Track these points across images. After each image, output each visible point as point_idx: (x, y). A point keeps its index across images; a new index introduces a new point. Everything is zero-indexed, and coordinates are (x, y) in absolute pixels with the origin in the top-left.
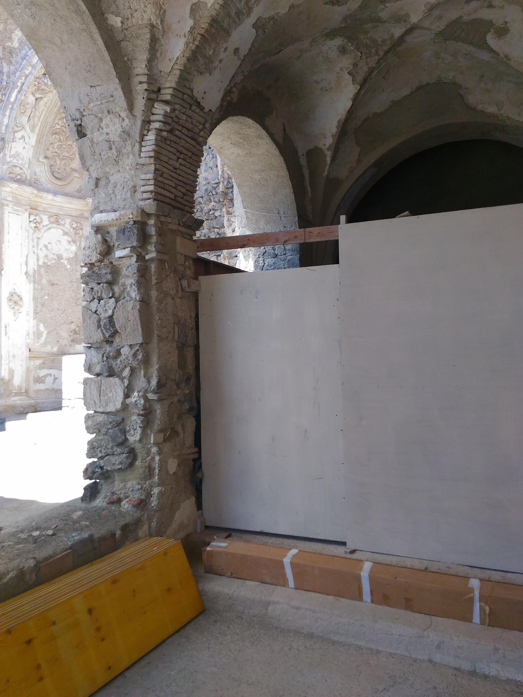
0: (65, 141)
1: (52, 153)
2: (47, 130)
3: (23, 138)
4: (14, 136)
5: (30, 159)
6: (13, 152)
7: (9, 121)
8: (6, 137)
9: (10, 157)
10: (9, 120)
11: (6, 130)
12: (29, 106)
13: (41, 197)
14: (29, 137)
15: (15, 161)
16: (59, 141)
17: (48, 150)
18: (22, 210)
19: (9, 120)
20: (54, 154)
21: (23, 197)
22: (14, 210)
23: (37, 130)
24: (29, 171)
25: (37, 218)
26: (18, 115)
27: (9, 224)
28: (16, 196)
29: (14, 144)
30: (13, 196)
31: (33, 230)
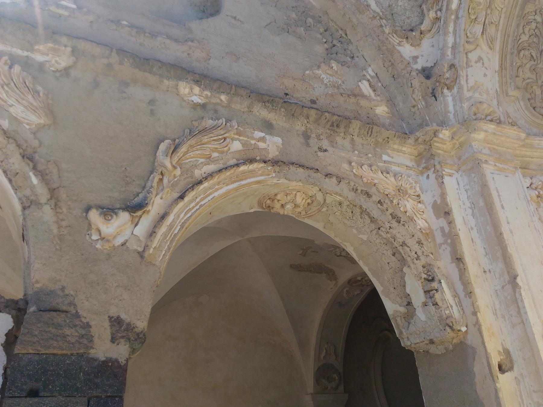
0: (539, 58)
1: (524, 80)
2: (509, 47)
3: (481, 61)
4: (467, 58)
5: (497, 90)
6: (471, 83)
7: (455, 39)
8: (456, 62)
9: (468, 91)
10: (455, 37)
11: (454, 54)
12: (481, 7)
13: (531, 147)
14: (489, 60)
15: (477, 95)
16: (530, 60)
17: (517, 76)
18: (509, 168)
19: (455, 37)
20: (529, 81)
21: (504, 149)
22: (497, 170)
23: (498, 45)
24: (501, 109)
25: (534, 181)
26: (467, 26)
27: (498, 192)
28: (494, 149)
29: (469, 70)
30: (489, 148)
31: (535, 202)
